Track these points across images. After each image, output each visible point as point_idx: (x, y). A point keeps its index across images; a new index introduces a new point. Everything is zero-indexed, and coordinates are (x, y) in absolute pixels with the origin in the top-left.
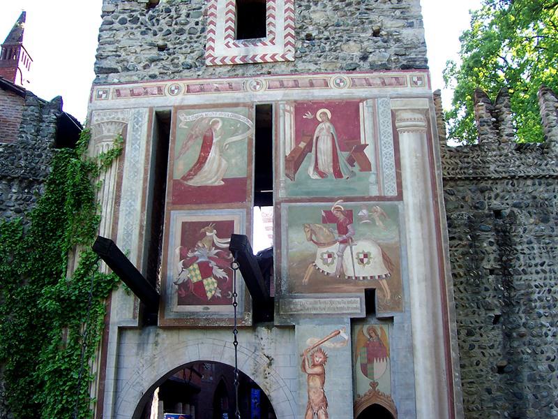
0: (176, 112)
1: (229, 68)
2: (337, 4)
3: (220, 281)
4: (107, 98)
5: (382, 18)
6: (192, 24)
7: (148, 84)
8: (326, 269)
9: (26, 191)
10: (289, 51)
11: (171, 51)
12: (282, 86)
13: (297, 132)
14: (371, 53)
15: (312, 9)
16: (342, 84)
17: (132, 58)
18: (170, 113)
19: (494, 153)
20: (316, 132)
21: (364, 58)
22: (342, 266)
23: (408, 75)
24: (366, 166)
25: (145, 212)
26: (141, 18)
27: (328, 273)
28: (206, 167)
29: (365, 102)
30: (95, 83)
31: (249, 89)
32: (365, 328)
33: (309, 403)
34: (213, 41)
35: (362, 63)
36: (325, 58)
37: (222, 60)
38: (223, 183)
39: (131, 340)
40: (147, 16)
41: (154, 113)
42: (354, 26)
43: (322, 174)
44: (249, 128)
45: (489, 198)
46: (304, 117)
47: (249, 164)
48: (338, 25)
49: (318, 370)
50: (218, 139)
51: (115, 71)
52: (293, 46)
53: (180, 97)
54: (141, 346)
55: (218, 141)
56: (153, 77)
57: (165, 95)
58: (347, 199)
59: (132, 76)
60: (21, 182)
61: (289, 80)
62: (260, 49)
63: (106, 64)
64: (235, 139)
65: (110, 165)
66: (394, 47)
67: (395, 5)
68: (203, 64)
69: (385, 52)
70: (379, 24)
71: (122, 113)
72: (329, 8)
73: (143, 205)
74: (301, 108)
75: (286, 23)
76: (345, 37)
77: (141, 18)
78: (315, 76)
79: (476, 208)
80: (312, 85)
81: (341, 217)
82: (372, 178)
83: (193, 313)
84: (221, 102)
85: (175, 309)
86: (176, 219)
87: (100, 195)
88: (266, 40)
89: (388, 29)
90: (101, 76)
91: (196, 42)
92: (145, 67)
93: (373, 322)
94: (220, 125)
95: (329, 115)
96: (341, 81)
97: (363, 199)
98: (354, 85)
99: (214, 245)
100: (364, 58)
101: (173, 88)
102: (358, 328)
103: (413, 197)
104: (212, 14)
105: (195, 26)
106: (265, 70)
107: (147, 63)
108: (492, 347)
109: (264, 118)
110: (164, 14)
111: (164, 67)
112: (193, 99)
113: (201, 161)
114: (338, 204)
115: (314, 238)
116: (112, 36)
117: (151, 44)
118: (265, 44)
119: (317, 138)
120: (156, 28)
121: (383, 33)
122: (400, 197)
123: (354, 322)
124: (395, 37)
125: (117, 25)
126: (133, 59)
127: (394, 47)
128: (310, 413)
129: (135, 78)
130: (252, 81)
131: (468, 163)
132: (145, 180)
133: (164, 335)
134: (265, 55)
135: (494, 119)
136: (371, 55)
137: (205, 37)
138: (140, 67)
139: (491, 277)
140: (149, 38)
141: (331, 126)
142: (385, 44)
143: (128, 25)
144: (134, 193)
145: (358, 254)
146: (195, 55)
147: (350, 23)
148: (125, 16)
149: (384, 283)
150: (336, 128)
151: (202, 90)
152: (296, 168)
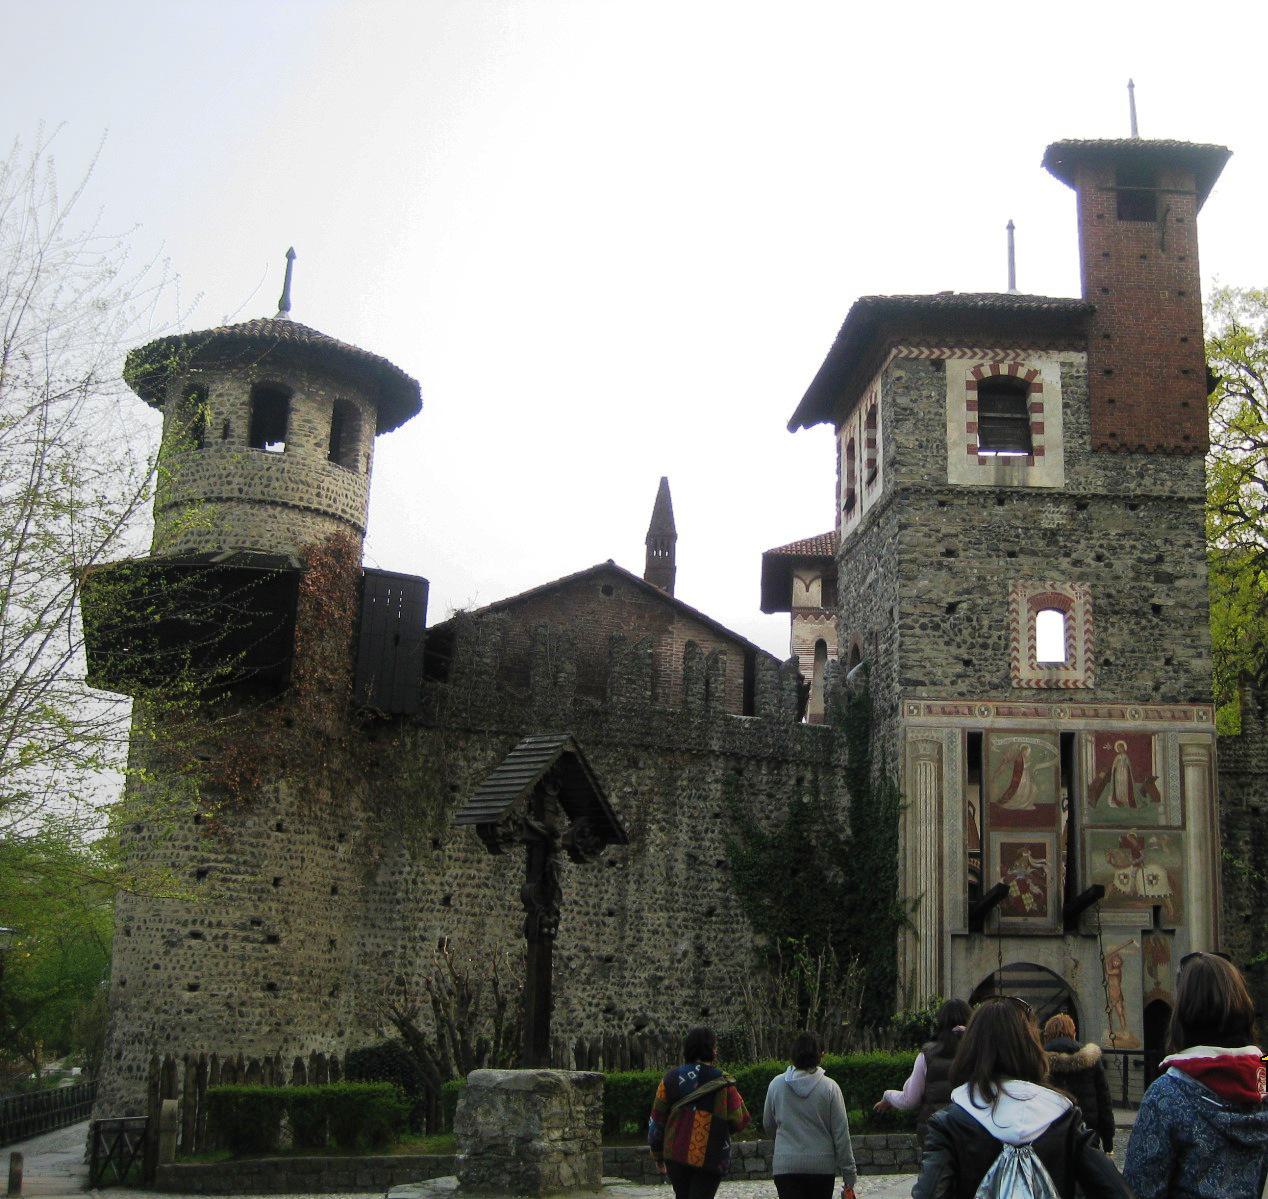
0: (987, 735)
3: (1037, 897)
4: (918, 714)
6: (994, 638)
7: (958, 703)
8: (1123, 888)
12: (1084, 715)
13: (1097, 760)
18: (981, 734)
21: (1156, 688)
23: (1195, 708)
24: (1156, 797)
28: (1019, 791)
32: (1152, 937)
34: (1018, 660)
39: (961, 944)
43: (1119, 803)
45: (1249, 794)
48: (1133, 651)
49: (1115, 971)
51: (922, 684)
53: (990, 719)
54: (969, 950)
56: (961, 694)
58: (1140, 827)
60: (769, 763)
63: (909, 675)
64: (1044, 765)
68: (1010, 684)
71: (936, 731)
74: (1103, 739)
76: (1140, 665)
79: (1236, 805)
80: (1110, 716)
81: (1135, 843)
84: (1028, 727)
90: (910, 688)
92: (953, 683)
98: (1147, 717)
99: (1029, 864)
103: (1193, 828)
108: (1241, 946)
110: (966, 624)
111: (972, 686)
112: (1003, 722)
113: (1015, 785)
114: (1133, 831)
120: (958, 639)
121: (1175, 662)
122: (1183, 826)
123: (1145, 932)
125: (918, 631)
126: (939, 673)
127: (1183, 678)
129: (944, 694)
133: (987, 942)
134: (1067, 681)
137: (1010, 655)
138: (947, 681)
140: (953, 650)
143: (929, 631)
147: (1145, 649)
151: (1010, 713)
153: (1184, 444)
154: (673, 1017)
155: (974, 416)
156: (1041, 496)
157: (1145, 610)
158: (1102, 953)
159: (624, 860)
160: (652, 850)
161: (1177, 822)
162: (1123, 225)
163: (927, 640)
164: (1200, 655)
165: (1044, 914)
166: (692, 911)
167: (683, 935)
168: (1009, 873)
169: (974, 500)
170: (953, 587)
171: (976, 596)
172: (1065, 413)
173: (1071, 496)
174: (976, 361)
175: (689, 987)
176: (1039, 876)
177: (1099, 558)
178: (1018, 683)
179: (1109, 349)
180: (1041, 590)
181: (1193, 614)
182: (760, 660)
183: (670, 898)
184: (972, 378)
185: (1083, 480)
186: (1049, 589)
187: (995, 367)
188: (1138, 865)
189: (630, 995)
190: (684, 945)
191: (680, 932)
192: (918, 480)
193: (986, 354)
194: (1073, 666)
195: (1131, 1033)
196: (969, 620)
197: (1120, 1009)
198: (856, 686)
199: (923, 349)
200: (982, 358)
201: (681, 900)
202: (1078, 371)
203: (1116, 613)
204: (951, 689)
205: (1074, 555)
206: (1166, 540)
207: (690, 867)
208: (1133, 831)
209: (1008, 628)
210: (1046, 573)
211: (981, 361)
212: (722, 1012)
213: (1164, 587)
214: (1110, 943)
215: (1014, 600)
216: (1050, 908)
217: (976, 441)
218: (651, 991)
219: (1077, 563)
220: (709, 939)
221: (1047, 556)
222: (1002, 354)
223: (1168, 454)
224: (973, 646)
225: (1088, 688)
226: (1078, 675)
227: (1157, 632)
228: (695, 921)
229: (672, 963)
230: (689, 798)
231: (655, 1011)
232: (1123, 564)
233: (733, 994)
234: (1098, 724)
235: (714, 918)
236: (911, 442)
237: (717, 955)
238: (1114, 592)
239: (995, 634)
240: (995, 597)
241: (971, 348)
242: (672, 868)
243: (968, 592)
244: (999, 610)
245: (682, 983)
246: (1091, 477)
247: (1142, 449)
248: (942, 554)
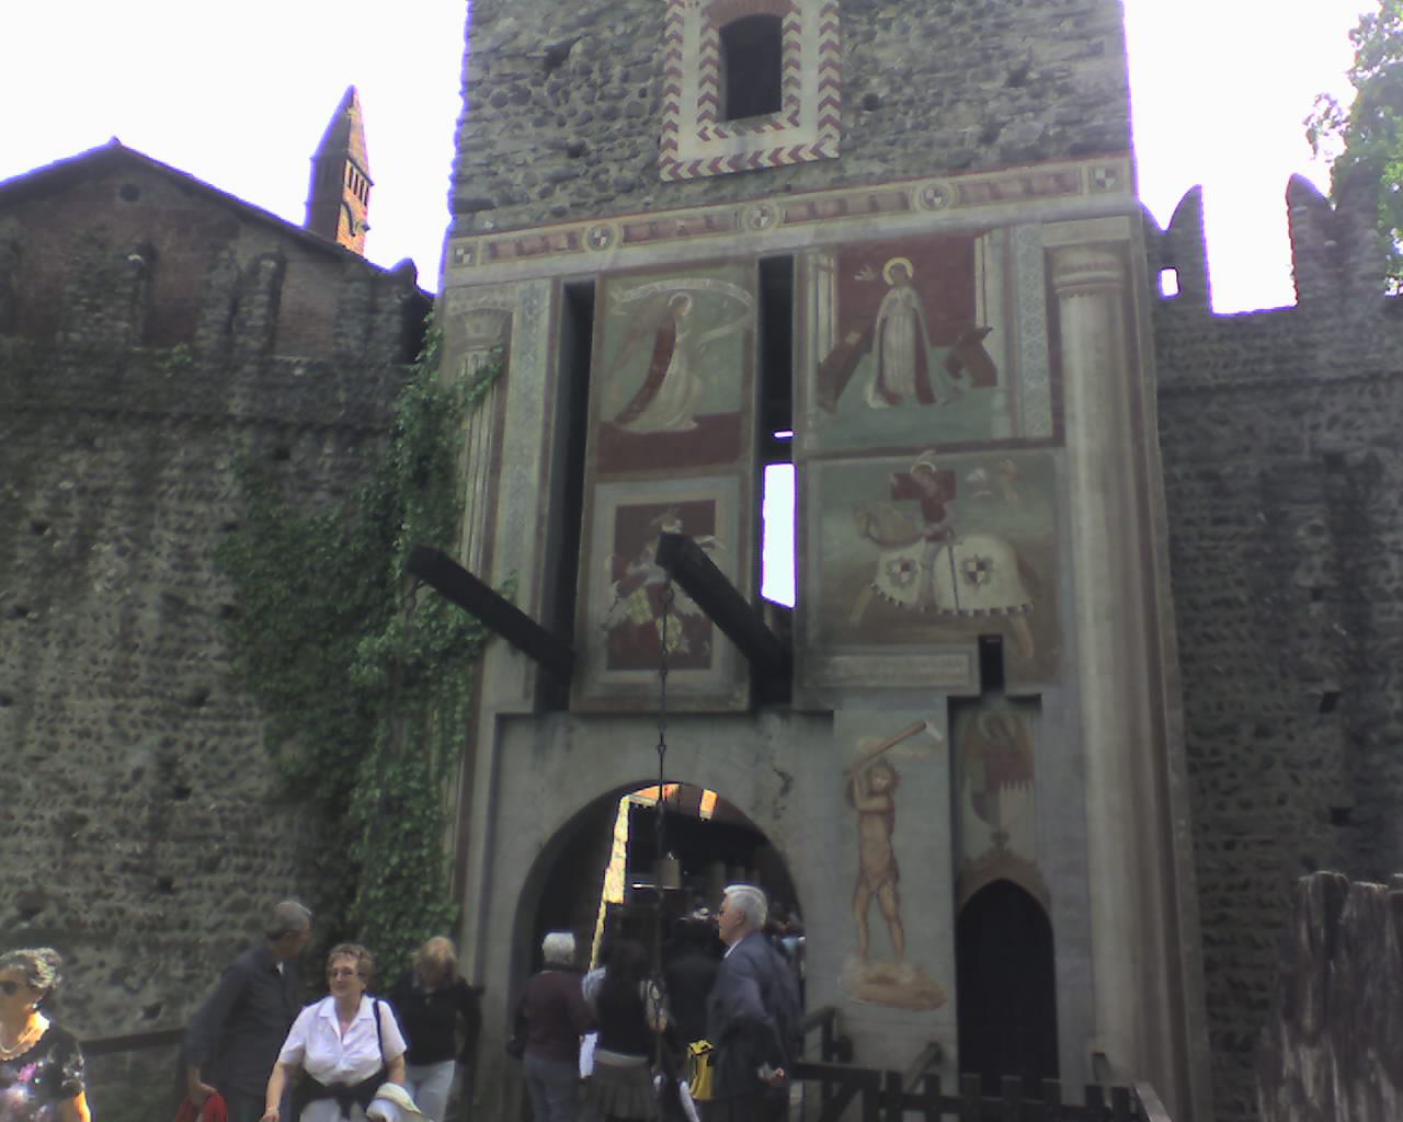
1: (706, 184)
2: (933, 21)
3: (689, 622)
4: (472, 261)
5: (1030, 40)
6: (634, 96)
8: (899, 595)
9: (350, 450)
10: (829, 136)
11: (594, 156)
12: (813, 214)
14: (1003, 124)
15: (877, 40)
16: (938, 201)
17: (518, 177)
19: (1329, 323)
20: (885, 302)
21: (988, 138)
22: (931, 587)
23: (1083, 167)
25: (548, 489)
26: (534, 91)
27: (901, 603)
28: (663, 393)
29: (986, 237)
30: (452, 234)
31: (745, 226)
33: (862, 871)
35: (983, 150)
36: (905, 145)
37: (693, 168)
38: (694, 425)
40: (546, 85)
41: (562, 289)
42: (968, 66)
43: (892, 398)
44: (744, 310)
45: (1315, 427)
46: (858, 278)
47: (746, 381)
48: (933, 69)
49: (879, 803)
50: (685, 335)
52: (837, 125)
53: (611, 251)
54: (540, 750)
57: (584, 251)
58: (943, 449)
59: (518, 213)
61: (825, 199)
62: (778, 139)
65: (480, 399)
66: (1055, 107)
68: (657, 179)
69: (1035, 119)
70: (1024, 58)
72: (914, 33)
73: (543, 474)
74: (853, 261)
75: (823, 77)
76: (948, 95)
77: (534, 91)
78: (881, 188)
79: (1282, 451)
80: (874, 207)
81: (931, 487)
82: (999, 401)
84: (689, 256)
85: (603, 679)
86: (607, 500)
87: (462, 458)
88: (782, 117)
89: (1046, 67)
91: (640, 134)
92: (544, 194)
93: (998, 705)
94: (689, 305)
95: (910, 271)
96: (937, 194)
97: (977, 446)
98: (964, 200)
101: (597, 235)
102: (965, 718)
105: (639, 100)
106: (780, 182)
107: (546, 185)
108: (1317, 764)
110: (579, 80)
112: (637, 255)
113: (654, 381)
114: (926, 459)
115: (873, 530)
116: (479, 133)
118: (778, 127)
119: (884, 321)
120: (562, 110)
121: (1033, 75)
122: (1058, 437)
123: (956, 705)
124: (1059, 82)
127: (1055, 107)
128: (863, 891)
129: (525, 218)
130: (751, 210)
131: (1263, 349)
132: (546, 425)
133: (582, 730)
134: (778, 151)
135: (1331, 243)
136: (1003, 131)
137: (660, 121)
138: (534, 193)
139: (1316, 608)
140: (551, 132)
141: (913, 294)
142: (1036, 102)
144: (525, 451)
145: (965, 563)
146: (638, 162)
148: (503, 89)
149: (1021, 623)
151: (654, 234)
154: (98, 894)
159: (44, 602)
161: (1038, 424)
166: (162, 695)
167: (138, 738)
175: (137, 837)
178: (673, 172)
188: (936, 538)
189: (18, 852)
190: (138, 757)
191: (132, 733)
197: (889, 902)
201: (143, 674)
204: (539, 206)
208: (926, 459)
209: (659, 73)
212: (199, 886)
215: (676, 17)
218: (59, 844)
220: (189, 747)
227: (990, 20)
228: (165, 713)
231: (62, 881)
233: (225, 851)
234: (843, 230)
235: (203, 710)
237: (203, 776)
242: (133, 620)
243: (589, 21)
245: (123, 829)
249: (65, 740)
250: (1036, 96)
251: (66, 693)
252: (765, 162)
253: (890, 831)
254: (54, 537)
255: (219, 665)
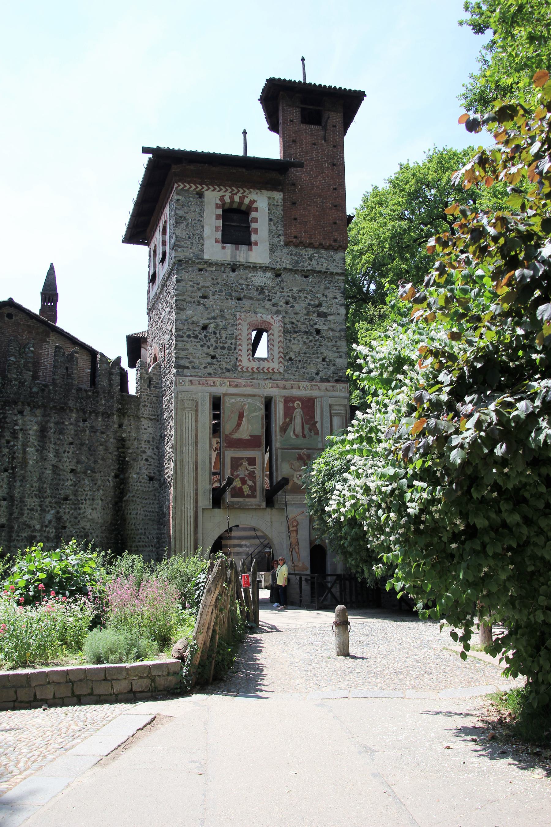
3: (251, 487)
11: (219, 360)
12: (278, 387)
13: (285, 413)
17: (197, 361)
21: (317, 374)
24: (317, 433)
26: (200, 336)
28: (241, 428)
37: (247, 369)
43: (297, 436)
47: (262, 428)
48: (305, 353)
49: (295, 528)
51: (188, 368)
53: (226, 388)
55: (247, 415)
58: (308, 449)
60: (103, 414)
61: (280, 383)
67: (334, 344)
68: (236, 370)
72: (301, 343)
74: (288, 400)
80: (292, 388)
81: (305, 457)
82: (320, 439)
83: (238, 502)
84: (247, 393)
90: (180, 370)
92: (205, 368)
97: (315, 449)
98: (312, 390)
99: (247, 469)
100: (317, 374)
104: (240, 339)
109: (268, 403)
110: (213, 336)
111: (215, 369)
112: (233, 390)
113: (239, 425)
114: (304, 451)
117: (207, 354)
120: (208, 344)
125: (185, 339)
127: (332, 368)
129: (199, 374)
130: (262, 382)
138: (202, 367)
140: (205, 349)
148: (190, 333)
150: (304, 412)
152: (285, 432)
153: (334, 244)
155: (220, 223)
156: (255, 267)
157: (312, 331)
158: (287, 516)
160: (31, 463)
162: (303, 126)
163: (191, 344)
164: (341, 357)
165: (255, 497)
166: (55, 497)
167: (49, 511)
168: (235, 473)
169: (218, 268)
170: (206, 315)
171: (218, 320)
172: (270, 224)
173: (274, 269)
174: (222, 193)
176: (252, 475)
177: (287, 303)
178: (242, 369)
179: (295, 191)
180: (255, 318)
181: (337, 334)
182: (99, 357)
183: (41, 490)
184: (219, 202)
185: (279, 260)
186: (260, 319)
187: (232, 198)
192: (187, 254)
193: (227, 190)
194: (272, 360)
195: (303, 563)
196: (215, 333)
198: (154, 374)
199: (192, 185)
200: (225, 192)
201: (48, 491)
202: (277, 202)
203: (296, 332)
205: (273, 301)
206: (323, 295)
207: (54, 472)
208: (304, 451)
209: (236, 339)
210: (258, 310)
211: (224, 194)
213: (321, 320)
214: (293, 512)
216: (258, 493)
217: (219, 235)
219: (274, 305)
221: (259, 300)
222: (236, 191)
223: (327, 248)
224: (216, 348)
225: (280, 373)
226: (275, 365)
227: (318, 343)
229: (42, 526)
230: (54, 433)
232: (300, 307)
234: (286, 392)
235: (68, 502)
236: (184, 235)
237: (70, 522)
238: (295, 321)
239: (229, 342)
240: (230, 321)
241: (219, 186)
242: (43, 473)
243: (215, 318)
244: (232, 328)
246: (283, 258)
247: (311, 245)
248: (200, 297)
249: (26, 512)
250: (328, 365)
251: (25, 497)
252: (265, 370)
253: (297, 534)
254: (14, 445)
255: (72, 488)
